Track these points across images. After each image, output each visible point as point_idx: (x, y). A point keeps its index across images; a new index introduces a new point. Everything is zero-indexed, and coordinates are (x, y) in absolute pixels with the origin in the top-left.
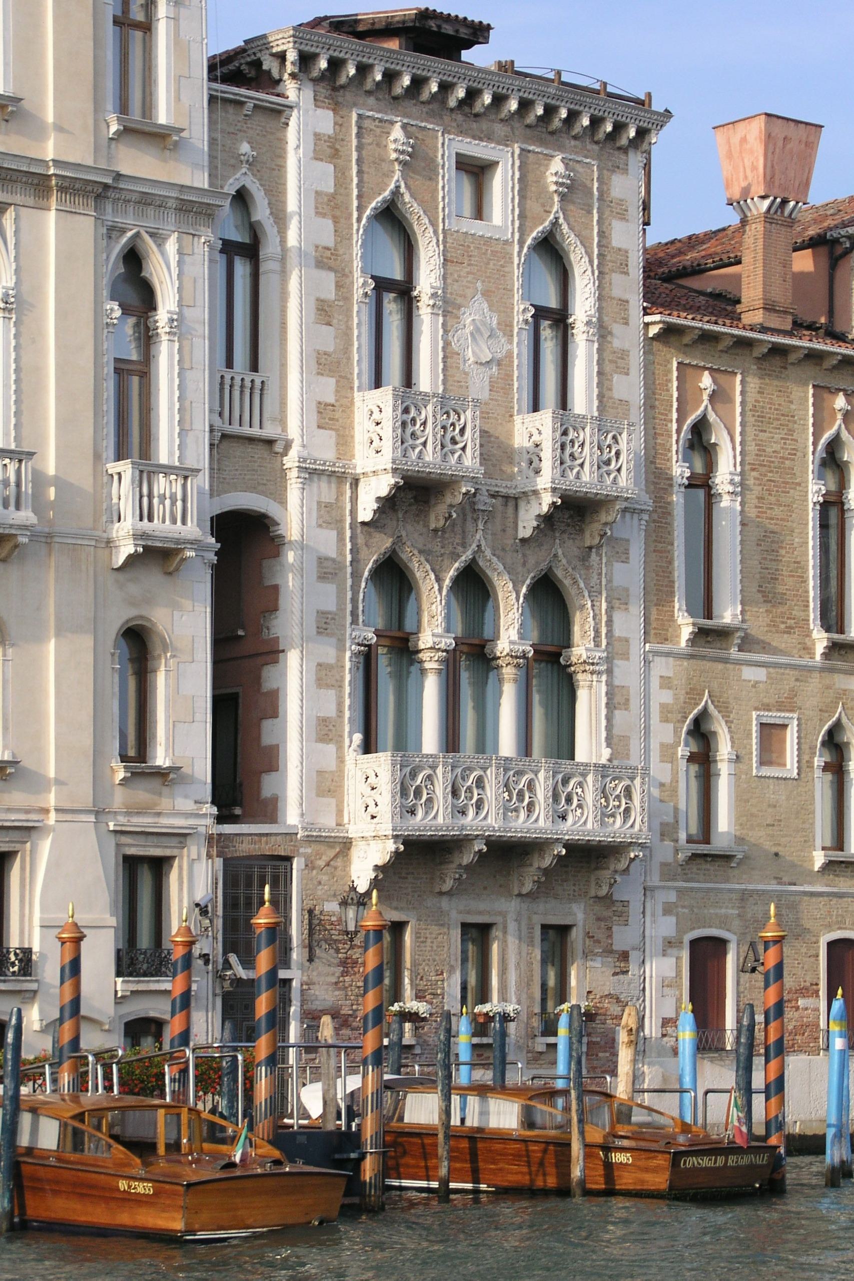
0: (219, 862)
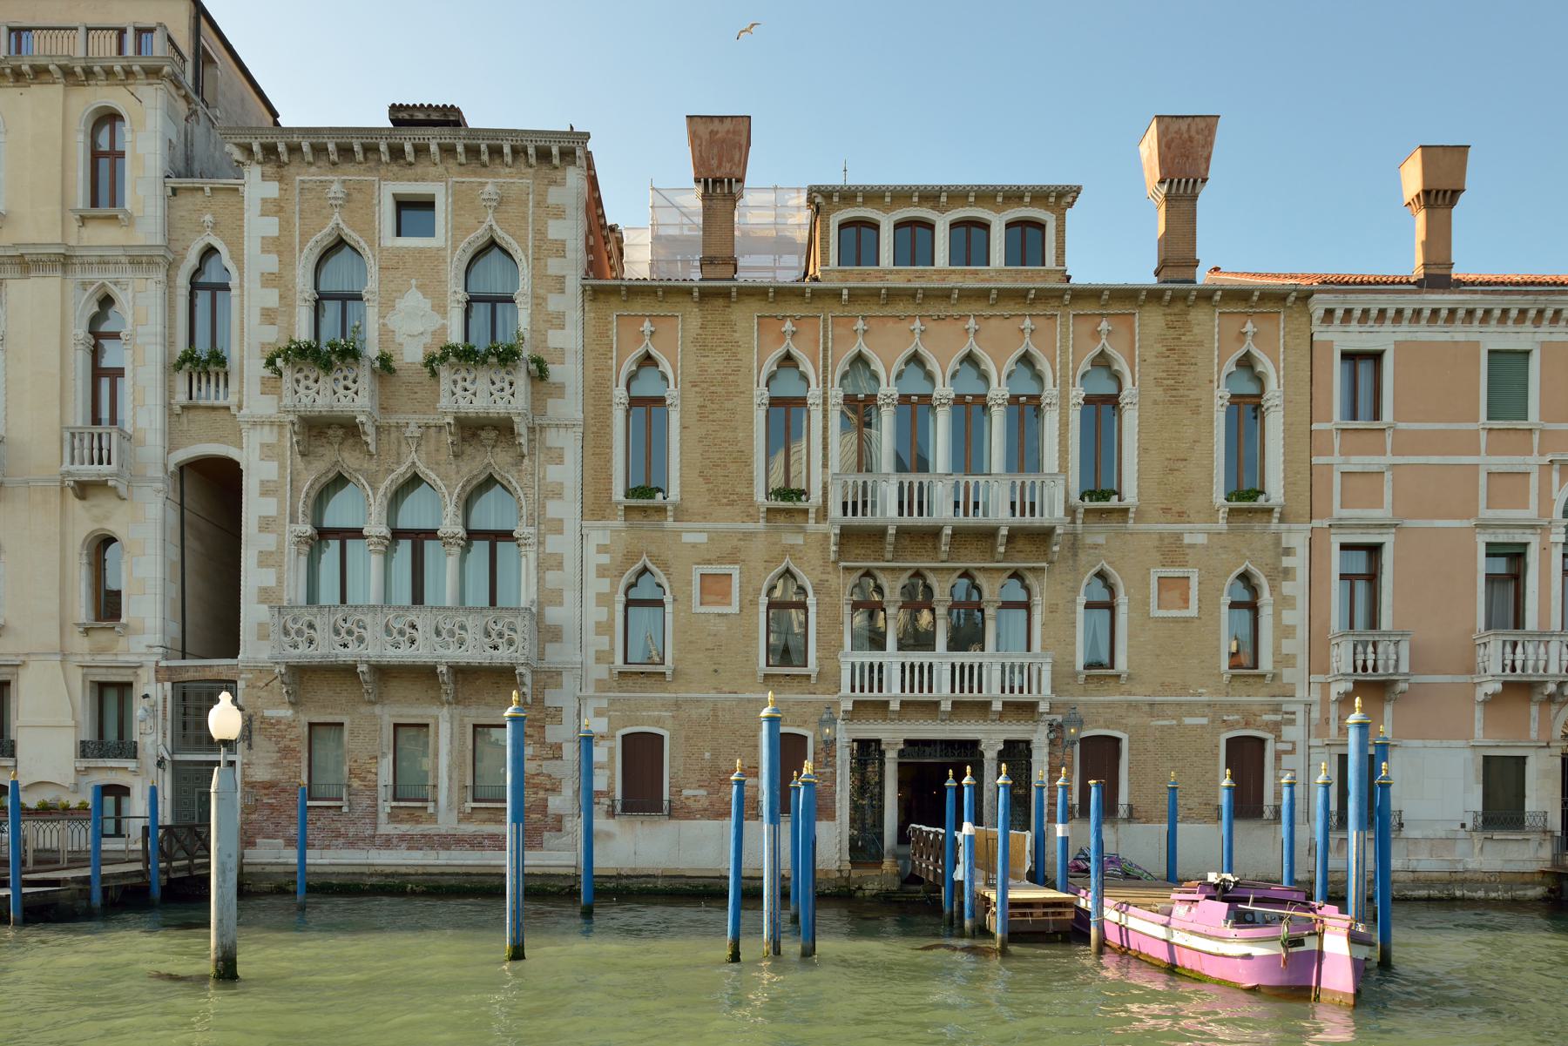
0: (168, 685)
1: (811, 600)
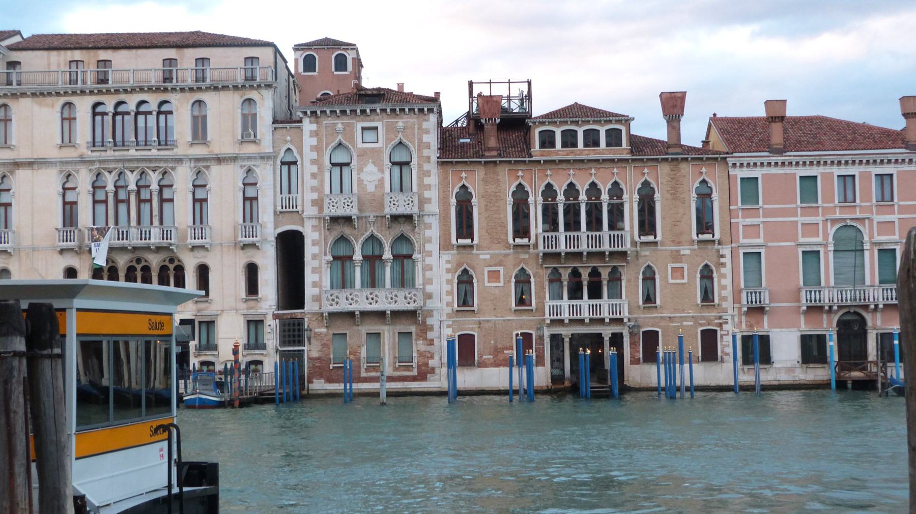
1: (532, 280)
